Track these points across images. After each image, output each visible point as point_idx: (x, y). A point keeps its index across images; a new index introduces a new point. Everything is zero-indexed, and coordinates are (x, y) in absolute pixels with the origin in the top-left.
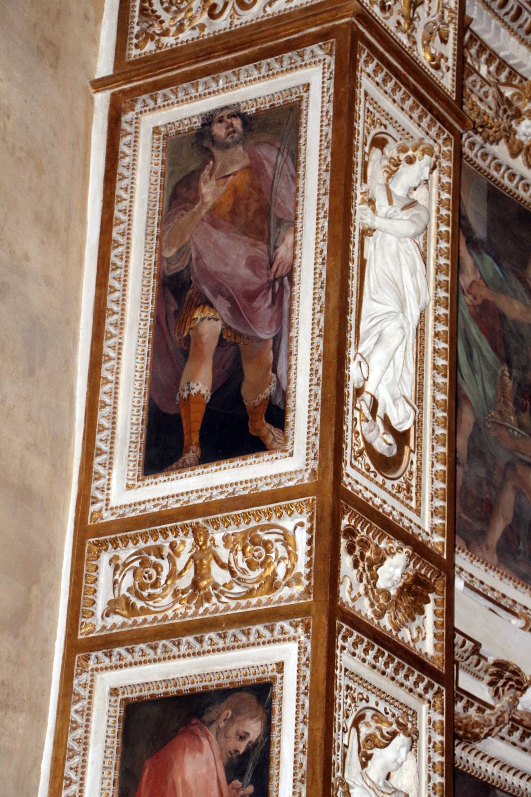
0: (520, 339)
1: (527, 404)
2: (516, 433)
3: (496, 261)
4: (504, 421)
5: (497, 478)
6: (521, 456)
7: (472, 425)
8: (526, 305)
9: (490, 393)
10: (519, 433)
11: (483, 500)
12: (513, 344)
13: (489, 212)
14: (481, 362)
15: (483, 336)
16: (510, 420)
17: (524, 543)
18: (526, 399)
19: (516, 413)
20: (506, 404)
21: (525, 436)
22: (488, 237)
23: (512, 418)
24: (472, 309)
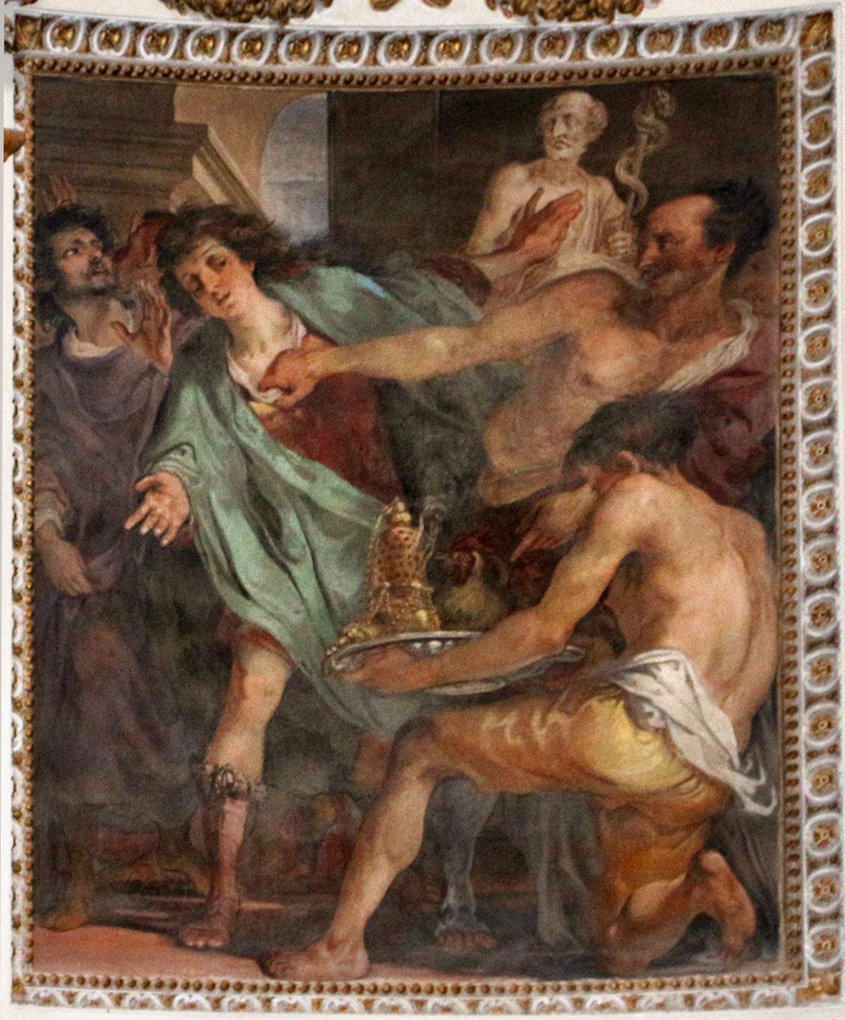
0: (450, 417)
1: (473, 559)
2: (435, 644)
3: (359, 267)
4: (395, 631)
5: (367, 774)
6: (451, 691)
7: (279, 690)
8: (468, 323)
9: (344, 585)
10: (443, 640)
11: (316, 846)
12: (425, 437)
13: (333, 160)
14: (312, 528)
15: (317, 467)
16: (418, 621)
17: (461, 889)
18: (469, 550)
19: (437, 598)
20: (399, 591)
21: (467, 639)
22: (335, 226)
23: (422, 615)
24: (279, 420)
